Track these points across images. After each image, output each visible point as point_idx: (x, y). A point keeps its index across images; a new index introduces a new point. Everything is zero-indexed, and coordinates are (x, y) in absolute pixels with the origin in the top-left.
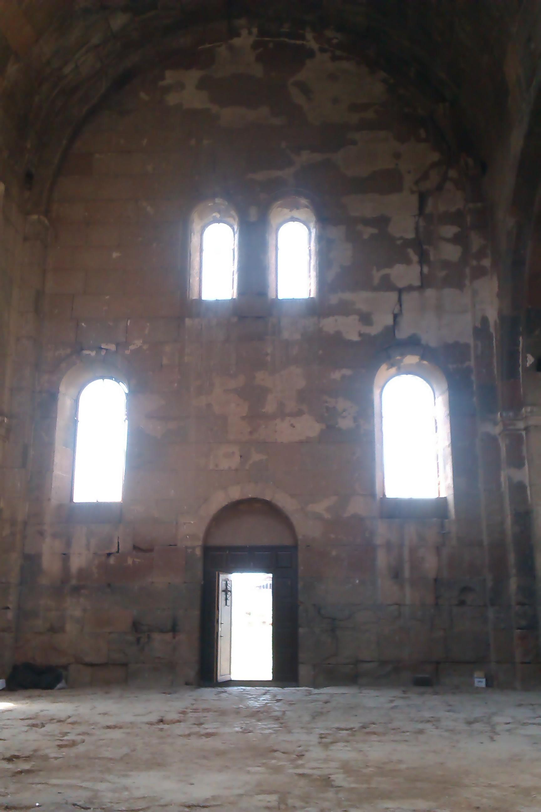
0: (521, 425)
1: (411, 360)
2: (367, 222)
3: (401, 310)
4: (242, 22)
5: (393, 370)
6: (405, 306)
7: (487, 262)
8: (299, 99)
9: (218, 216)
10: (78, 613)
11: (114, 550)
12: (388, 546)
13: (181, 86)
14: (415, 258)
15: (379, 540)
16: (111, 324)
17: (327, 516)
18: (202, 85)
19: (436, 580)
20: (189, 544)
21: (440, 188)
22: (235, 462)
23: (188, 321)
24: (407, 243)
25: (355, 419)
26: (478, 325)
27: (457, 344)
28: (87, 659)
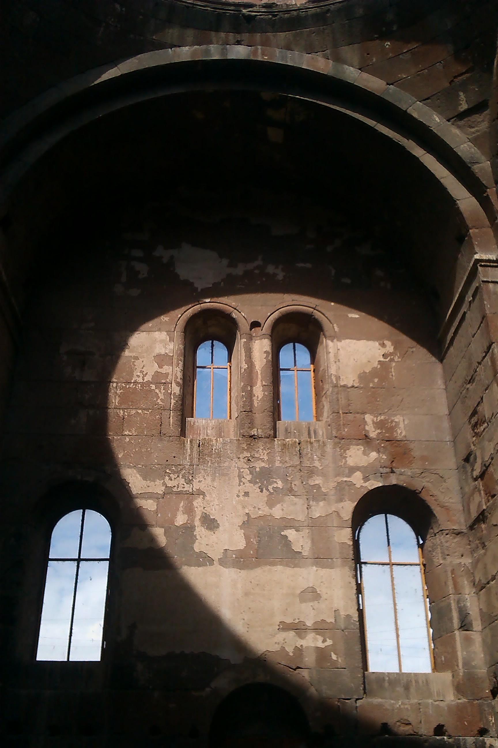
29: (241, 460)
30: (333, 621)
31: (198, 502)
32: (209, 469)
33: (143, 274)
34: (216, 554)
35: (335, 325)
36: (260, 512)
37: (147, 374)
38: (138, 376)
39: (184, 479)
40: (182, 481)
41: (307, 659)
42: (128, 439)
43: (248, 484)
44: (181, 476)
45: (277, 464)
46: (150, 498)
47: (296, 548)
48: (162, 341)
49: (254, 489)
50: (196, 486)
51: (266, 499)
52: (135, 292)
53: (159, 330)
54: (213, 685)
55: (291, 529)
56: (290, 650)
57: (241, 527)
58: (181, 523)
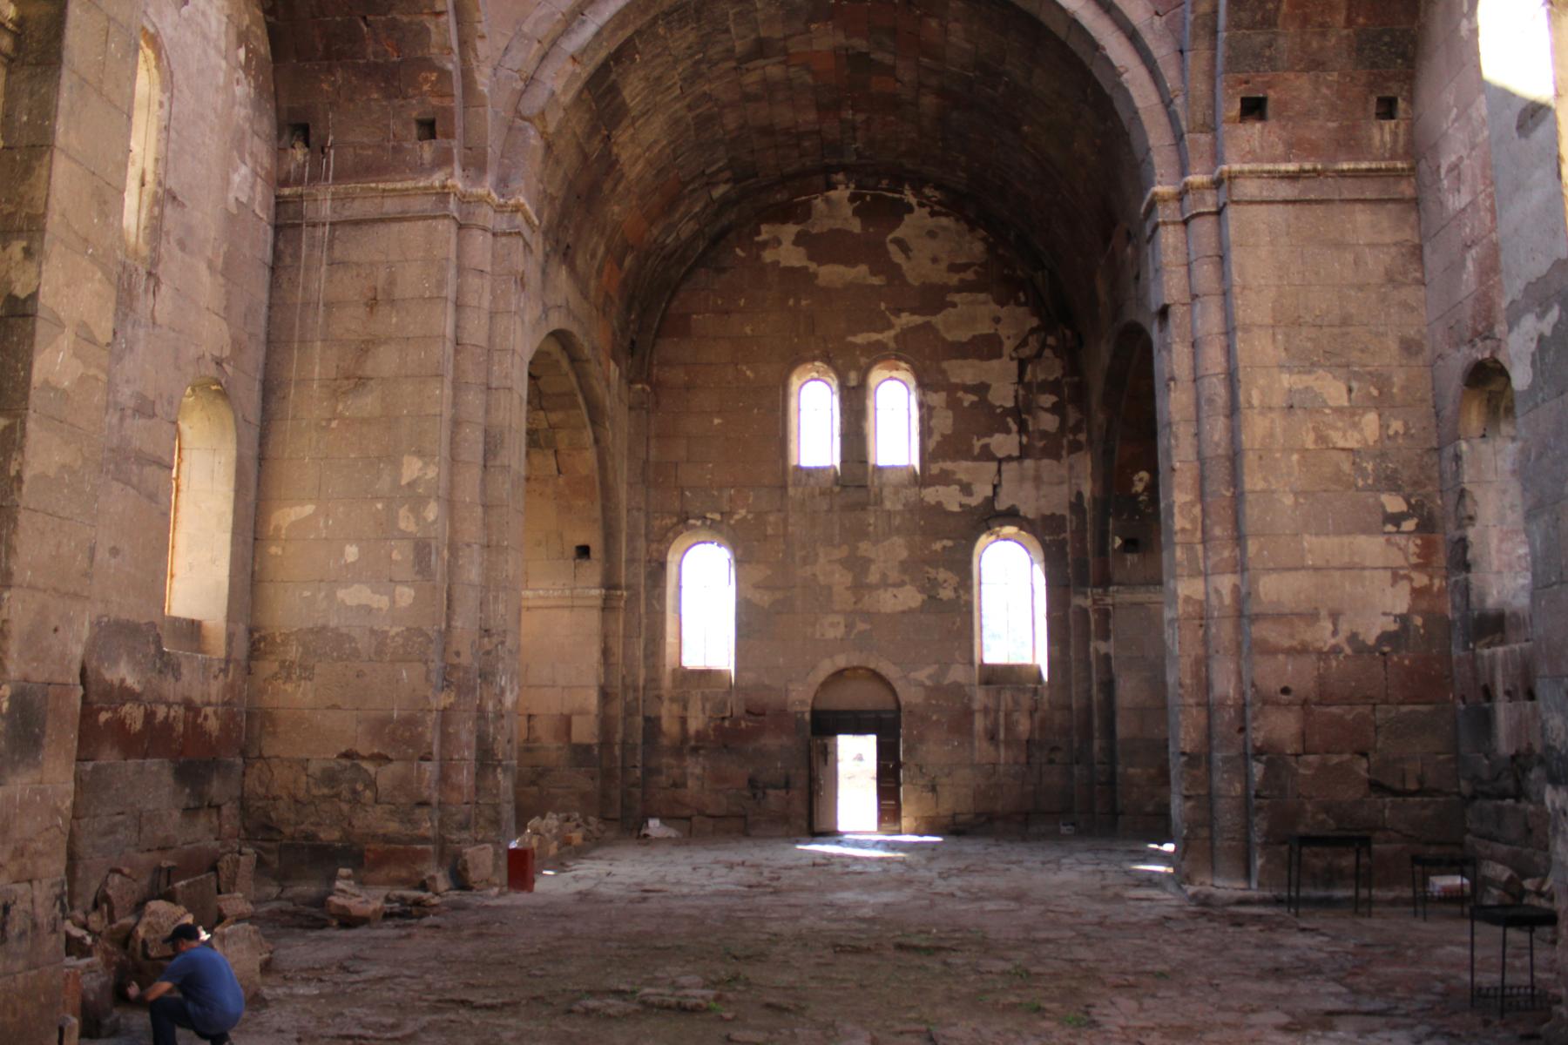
0: (1109, 600)
1: (1010, 530)
2: (967, 389)
3: (1000, 481)
4: (840, 177)
5: (993, 538)
6: (1004, 475)
7: (1082, 437)
8: (897, 257)
9: (815, 375)
10: (698, 771)
11: (728, 714)
12: (986, 711)
13: (777, 242)
14: (1014, 427)
15: (976, 706)
16: (716, 493)
17: (928, 683)
18: (799, 240)
19: (1028, 741)
20: (798, 708)
21: (1039, 355)
22: (840, 632)
23: (791, 491)
24: (1007, 412)
25: (956, 590)
26: (1073, 499)
27: (1053, 515)
28: (708, 812)
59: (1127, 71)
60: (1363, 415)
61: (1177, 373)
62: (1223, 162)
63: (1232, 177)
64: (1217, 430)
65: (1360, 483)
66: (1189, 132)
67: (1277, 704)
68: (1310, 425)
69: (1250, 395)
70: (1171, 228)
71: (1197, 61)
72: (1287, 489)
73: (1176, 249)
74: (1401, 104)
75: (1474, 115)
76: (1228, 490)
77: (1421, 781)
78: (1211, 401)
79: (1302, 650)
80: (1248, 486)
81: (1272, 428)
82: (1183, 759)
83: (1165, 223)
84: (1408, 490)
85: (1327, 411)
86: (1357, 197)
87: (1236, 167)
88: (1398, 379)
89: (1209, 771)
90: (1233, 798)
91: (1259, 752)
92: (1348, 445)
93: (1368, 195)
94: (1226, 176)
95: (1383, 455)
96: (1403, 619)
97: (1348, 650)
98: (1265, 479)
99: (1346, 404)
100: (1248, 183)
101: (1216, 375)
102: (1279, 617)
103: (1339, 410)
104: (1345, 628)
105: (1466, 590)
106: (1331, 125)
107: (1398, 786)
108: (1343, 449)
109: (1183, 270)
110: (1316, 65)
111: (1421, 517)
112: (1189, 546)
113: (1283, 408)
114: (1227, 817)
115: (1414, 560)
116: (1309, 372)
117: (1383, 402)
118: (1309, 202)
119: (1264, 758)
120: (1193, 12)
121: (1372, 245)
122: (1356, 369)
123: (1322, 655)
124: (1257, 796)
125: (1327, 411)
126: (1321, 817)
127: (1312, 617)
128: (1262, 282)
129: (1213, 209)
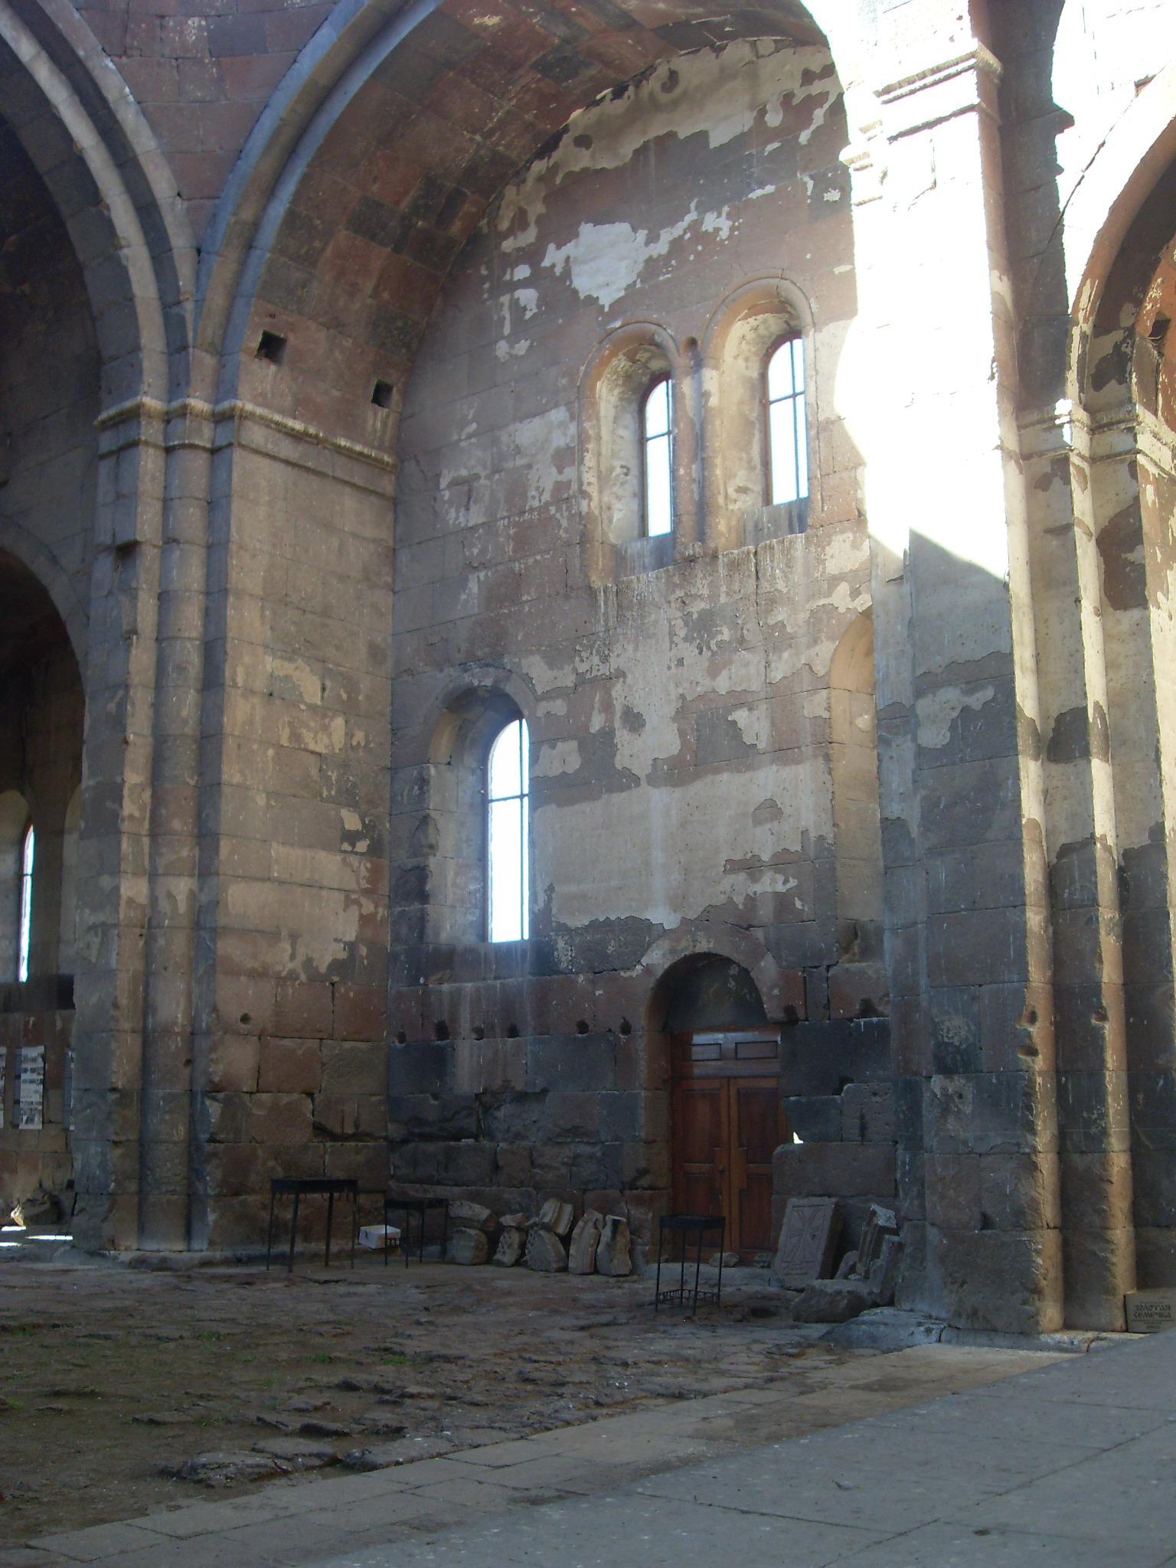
29: (673, 604)
30: (799, 848)
31: (617, 690)
32: (629, 632)
33: (531, 310)
34: (641, 769)
35: (812, 300)
36: (699, 689)
37: (543, 491)
38: (533, 497)
39: (598, 657)
40: (596, 660)
41: (761, 912)
42: (527, 609)
43: (682, 645)
44: (594, 652)
45: (723, 599)
46: (557, 697)
47: (748, 740)
48: (561, 424)
49: (689, 651)
50: (615, 663)
51: (707, 664)
52: (522, 347)
53: (556, 406)
54: (644, 961)
55: (741, 708)
56: (739, 900)
57: (674, 719)
58: (597, 728)
59: (129, 246)
60: (332, 719)
61: (140, 626)
62: (236, 396)
63: (245, 416)
64: (186, 704)
65: (325, 793)
66: (194, 347)
67: (237, 1033)
68: (286, 719)
69: (235, 672)
70: (151, 451)
71: (222, 270)
72: (261, 788)
73: (153, 478)
74: (395, 396)
75: (504, 439)
76: (192, 778)
77: (357, 1125)
78: (181, 669)
79: (258, 974)
80: (225, 777)
81: (251, 714)
82: (112, 1097)
83: (147, 443)
84: (363, 807)
85: (303, 707)
86: (347, 478)
87: (249, 407)
88: (365, 685)
89: (143, 1113)
90: (175, 1143)
91: (214, 1090)
92: (318, 750)
93: (357, 480)
94: (238, 413)
95: (345, 766)
96: (351, 947)
97: (303, 977)
98: (243, 775)
99: (319, 703)
100: (256, 428)
101: (189, 639)
102: (244, 933)
103: (312, 708)
104: (302, 952)
105: (422, 919)
106: (336, 393)
107: (338, 1130)
108: (312, 752)
109: (158, 505)
110: (336, 324)
111: (372, 839)
112: (136, 837)
113: (264, 694)
114: (169, 1165)
115: (364, 884)
116: (291, 660)
117: (349, 709)
118: (308, 470)
119: (221, 1095)
120: (235, 214)
121: (355, 536)
122: (331, 666)
123: (281, 980)
124: (212, 1140)
125: (303, 707)
126: (271, 1163)
127: (274, 936)
128: (258, 545)
129: (208, 446)
